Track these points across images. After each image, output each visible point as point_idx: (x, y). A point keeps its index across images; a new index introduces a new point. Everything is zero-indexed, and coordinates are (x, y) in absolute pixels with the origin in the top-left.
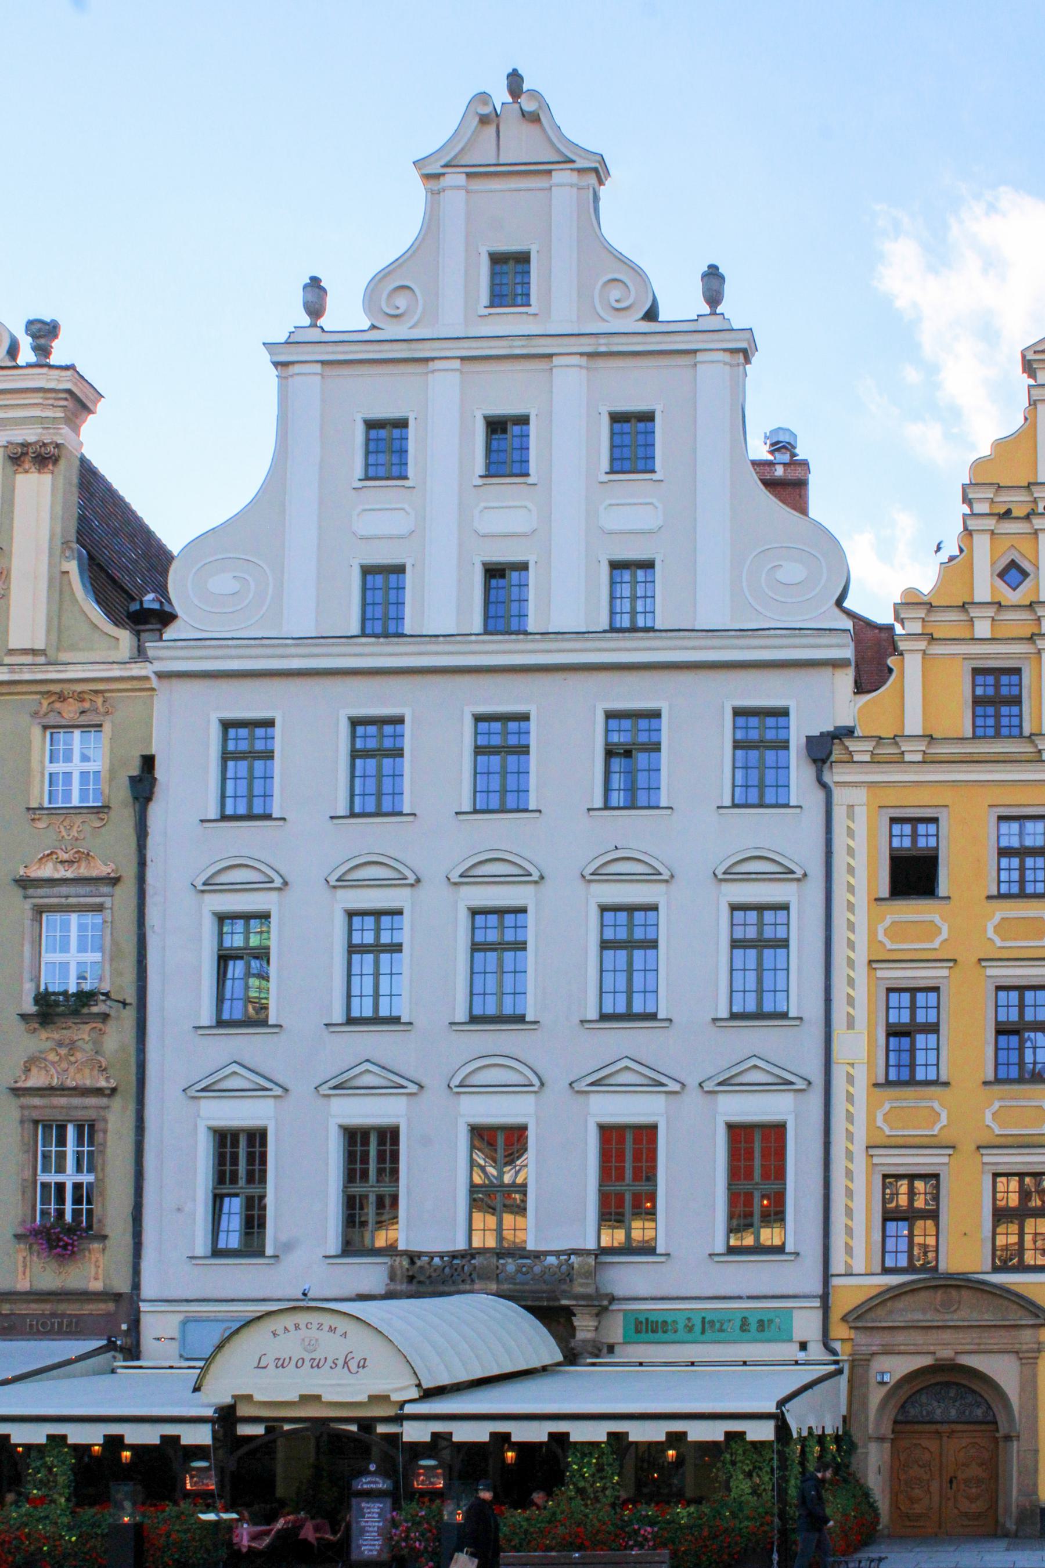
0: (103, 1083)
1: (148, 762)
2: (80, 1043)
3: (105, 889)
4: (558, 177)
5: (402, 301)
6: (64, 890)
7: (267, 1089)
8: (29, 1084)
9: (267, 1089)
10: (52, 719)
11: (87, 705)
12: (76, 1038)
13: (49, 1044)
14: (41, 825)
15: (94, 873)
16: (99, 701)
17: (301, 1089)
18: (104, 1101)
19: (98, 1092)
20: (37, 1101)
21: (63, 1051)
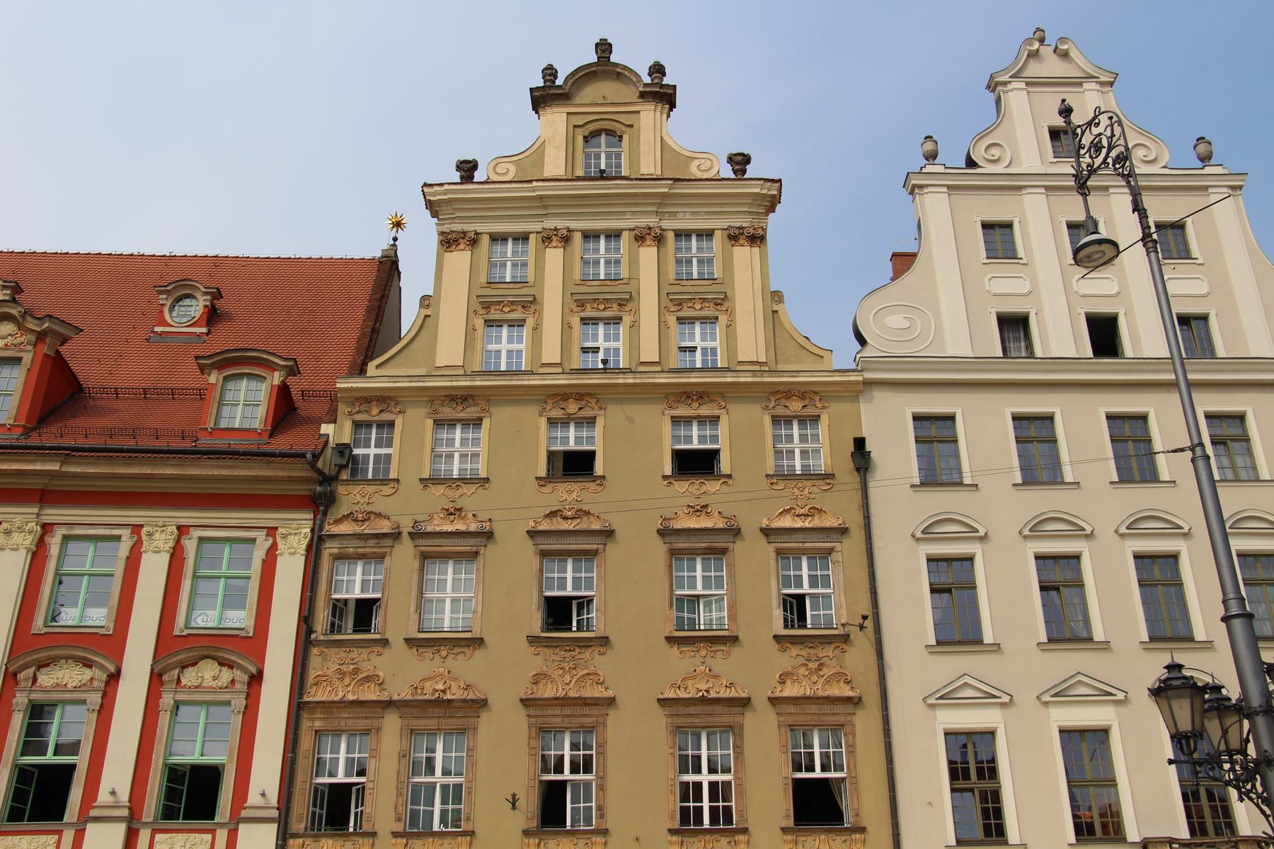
0: (851, 694)
1: (860, 443)
2: (825, 660)
3: (835, 536)
4: (1086, 86)
5: (995, 152)
6: (800, 537)
7: (995, 697)
8: (786, 694)
9: (995, 697)
10: (780, 411)
11: (807, 402)
12: (821, 655)
13: (801, 661)
14: (775, 487)
15: (828, 524)
16: (817, 398)
17: (1026, 697)
18: (850, 708)
19: (849, 700)
20: (791, 709)
21: (813, 665)
